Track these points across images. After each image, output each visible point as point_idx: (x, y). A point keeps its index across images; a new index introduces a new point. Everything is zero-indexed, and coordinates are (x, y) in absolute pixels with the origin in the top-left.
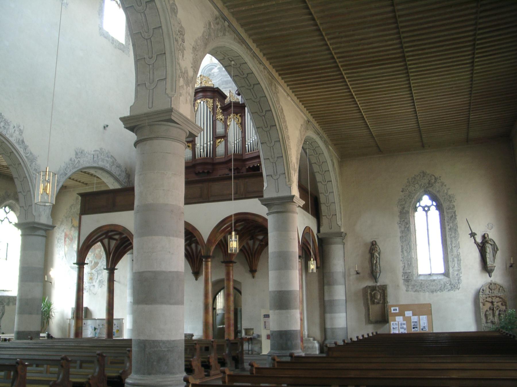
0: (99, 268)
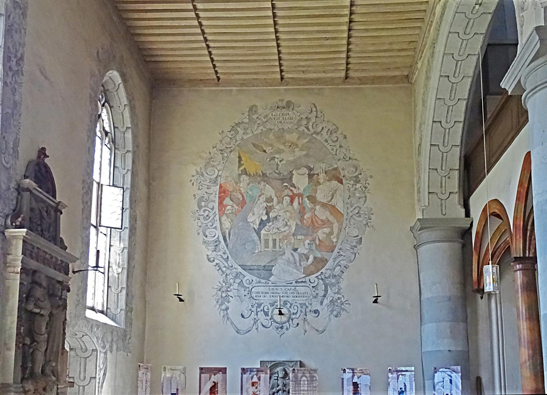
0: (329, 272)
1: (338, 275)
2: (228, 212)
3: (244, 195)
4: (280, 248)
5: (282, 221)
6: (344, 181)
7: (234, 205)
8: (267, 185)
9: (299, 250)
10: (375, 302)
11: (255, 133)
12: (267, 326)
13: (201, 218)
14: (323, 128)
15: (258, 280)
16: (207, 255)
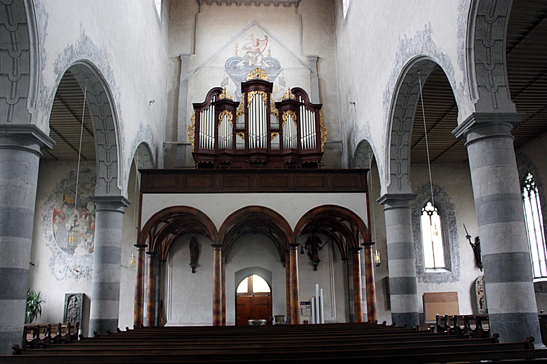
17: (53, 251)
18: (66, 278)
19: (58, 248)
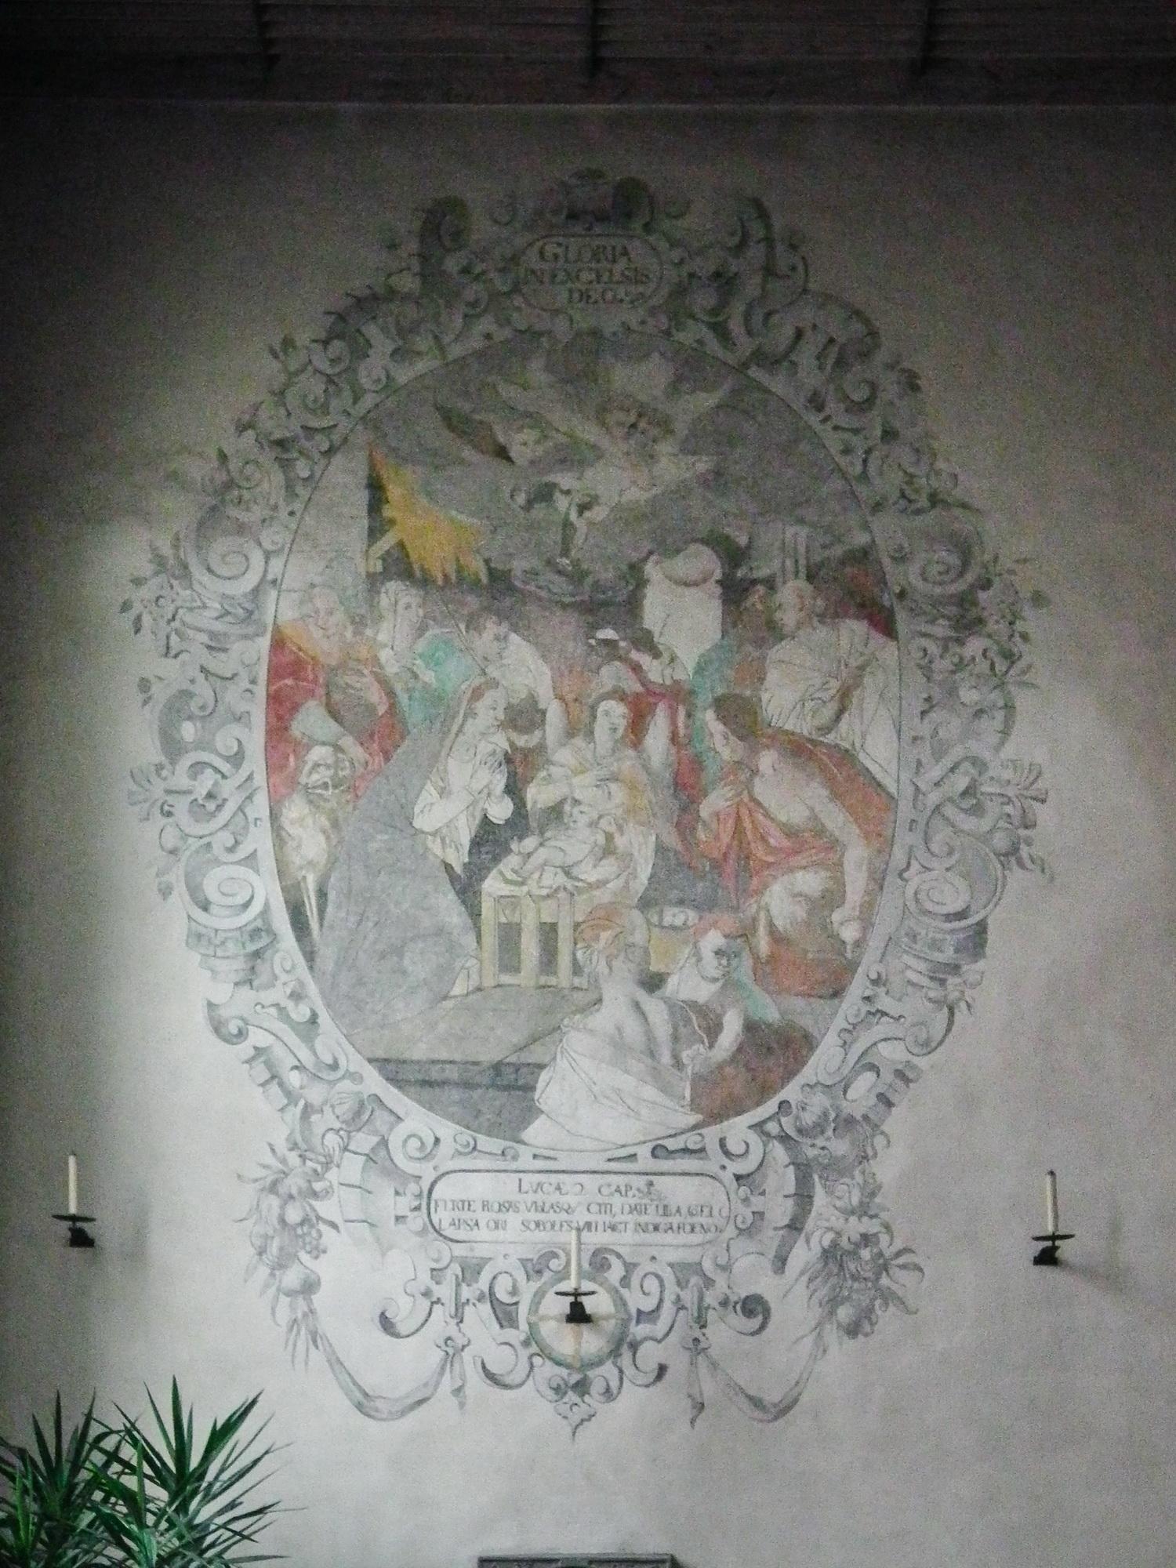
0: (819, 1102)
1: (866, 1117)
2: (315, 777)
3: (398, 688)
4: (577, 969)
5: (587, 832)
6: (903, 622)
7: (348, 742)
8: (514, 637)
9: (672, 983)
10: (1047, 1258)
11: (456, 351)
12: (508, 1380)
13: (181, 805)
14: (799, 334)
15: (466, 1136)
16: (211, 1006)
17: (291, 1096)
18: (458, 1391)
19: (353, 1061)
